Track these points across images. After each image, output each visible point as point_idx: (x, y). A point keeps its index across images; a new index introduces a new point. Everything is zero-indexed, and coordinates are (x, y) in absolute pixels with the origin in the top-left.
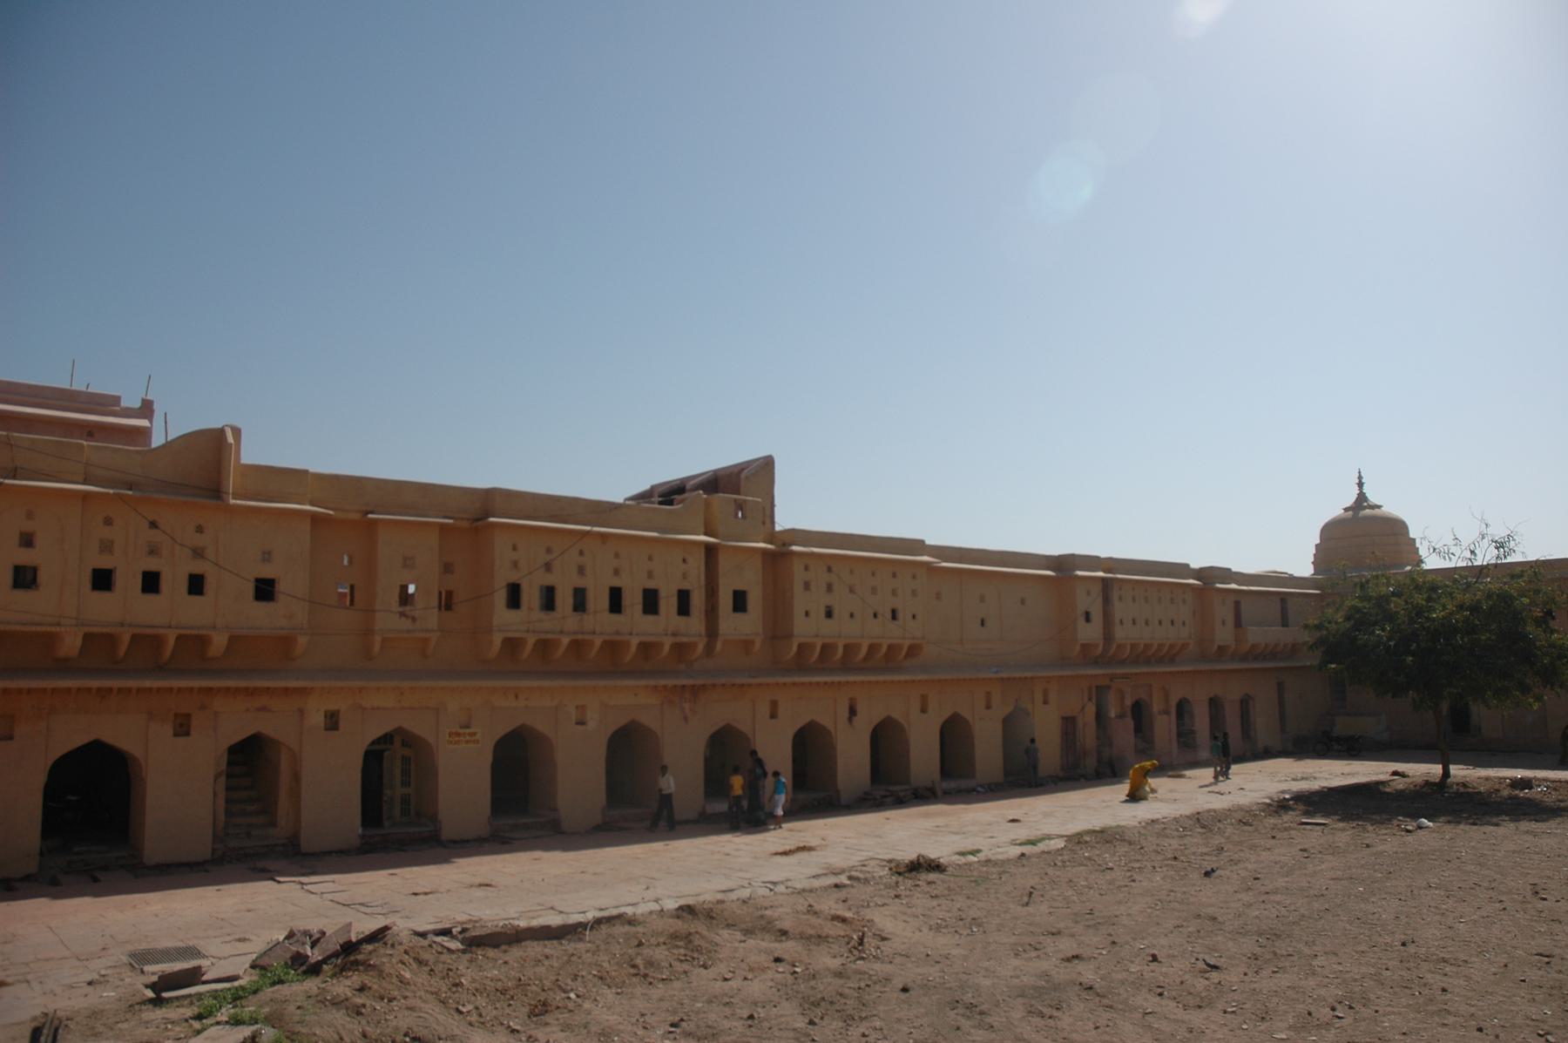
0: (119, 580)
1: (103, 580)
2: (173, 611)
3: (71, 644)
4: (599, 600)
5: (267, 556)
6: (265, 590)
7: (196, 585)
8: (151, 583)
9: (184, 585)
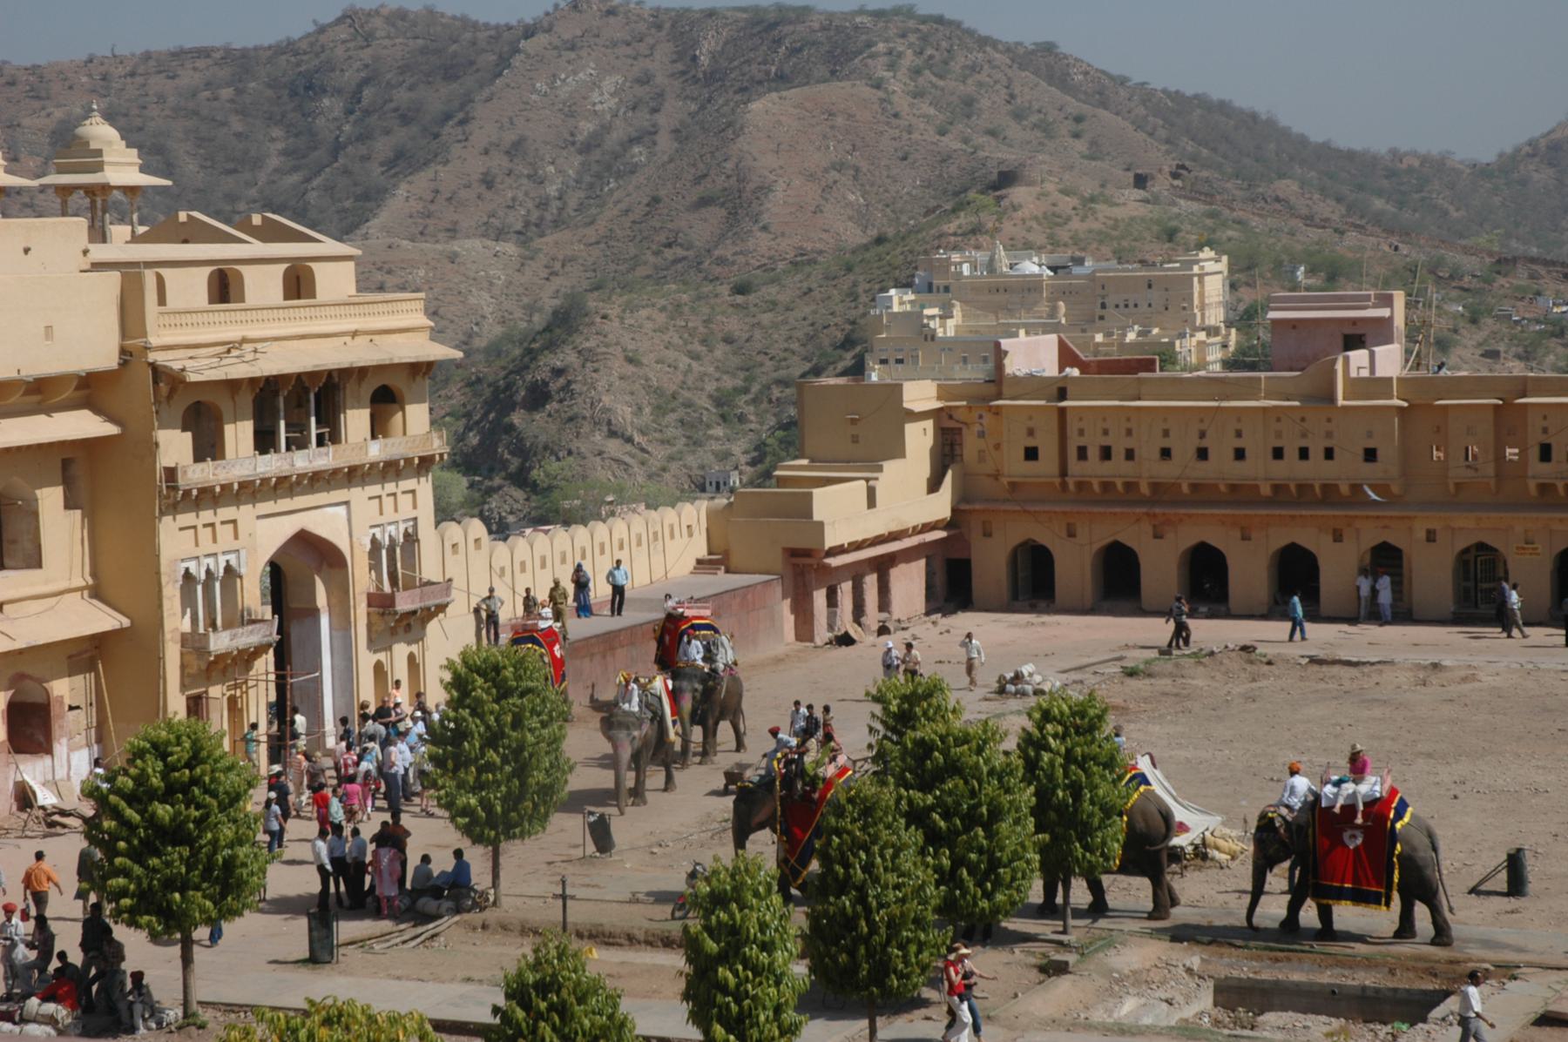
0: (1286, 452)
1: (1278, 453)
2: (1316, 470)
3: (1266, 490)
5: (1370, 435)
6: (1370, 455)
7: (1329, 454)
8: (1304, 454)
9: (1322, 455)
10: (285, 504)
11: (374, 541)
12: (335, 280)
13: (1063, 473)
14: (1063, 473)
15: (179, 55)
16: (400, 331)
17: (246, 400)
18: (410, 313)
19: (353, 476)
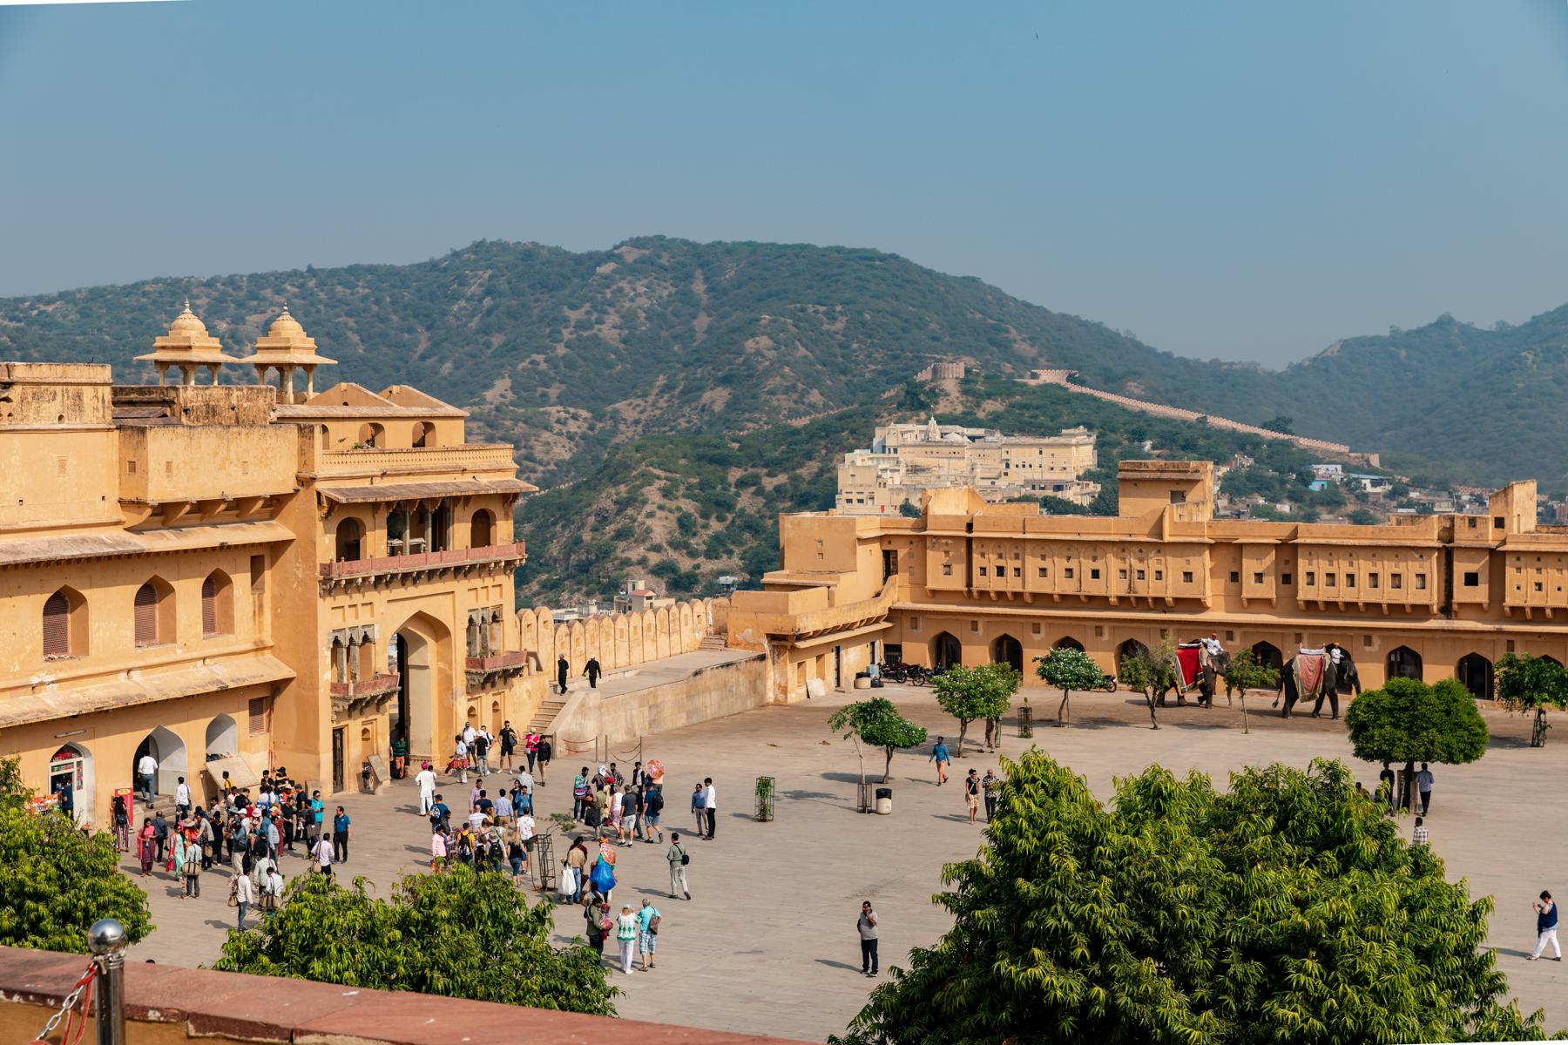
4: (1363, 579)
10: (412, 591)
11: (471, 621)
12: (450, 433)
13: (969, 584)
14: (969, 584)
15: (353, 270)
16: (493, 469)
17: (383, 515)
18: (504, 456)
19: (459, 572)
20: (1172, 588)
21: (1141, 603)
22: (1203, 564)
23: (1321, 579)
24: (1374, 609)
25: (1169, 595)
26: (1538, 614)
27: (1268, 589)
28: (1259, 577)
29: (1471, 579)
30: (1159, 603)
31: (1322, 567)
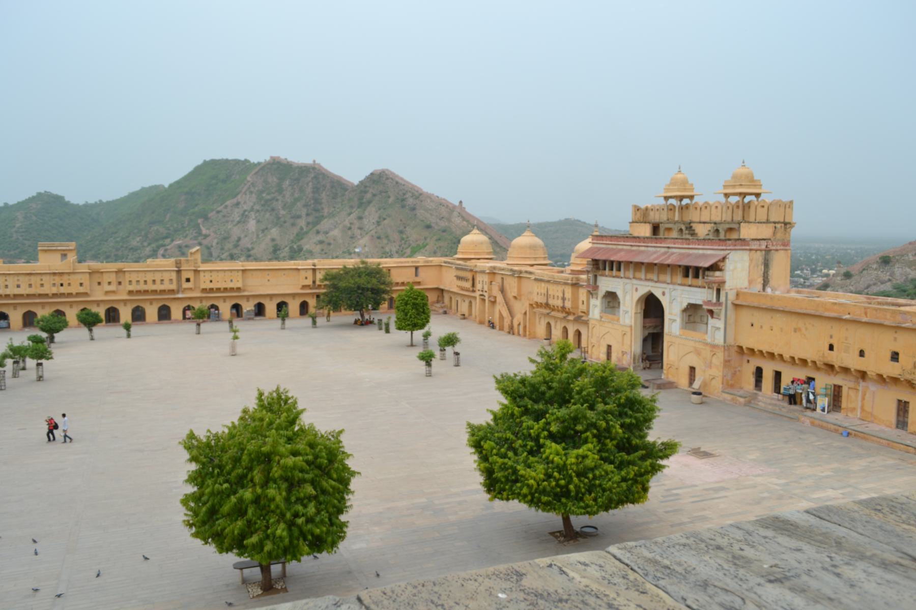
4: (150, 282)
20: (74, 289)
21: (62, 295)
22: (85, 279)
23: (134, 283)
24: (154, 292)
25: (74, 292)
26: (211, 290)
27: (112, 288)
28: (109, 283)
29: (188, 280)
30: (70, 295)
31: (134, 277)
